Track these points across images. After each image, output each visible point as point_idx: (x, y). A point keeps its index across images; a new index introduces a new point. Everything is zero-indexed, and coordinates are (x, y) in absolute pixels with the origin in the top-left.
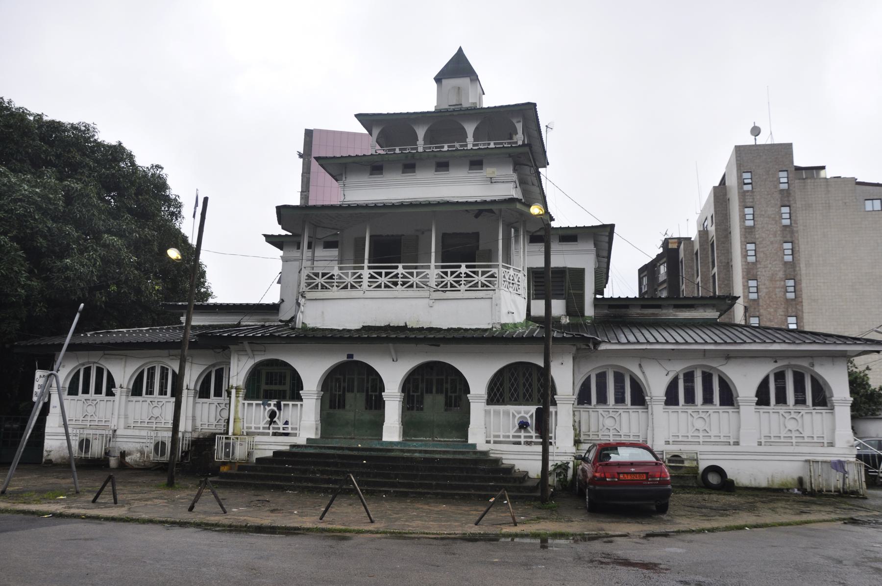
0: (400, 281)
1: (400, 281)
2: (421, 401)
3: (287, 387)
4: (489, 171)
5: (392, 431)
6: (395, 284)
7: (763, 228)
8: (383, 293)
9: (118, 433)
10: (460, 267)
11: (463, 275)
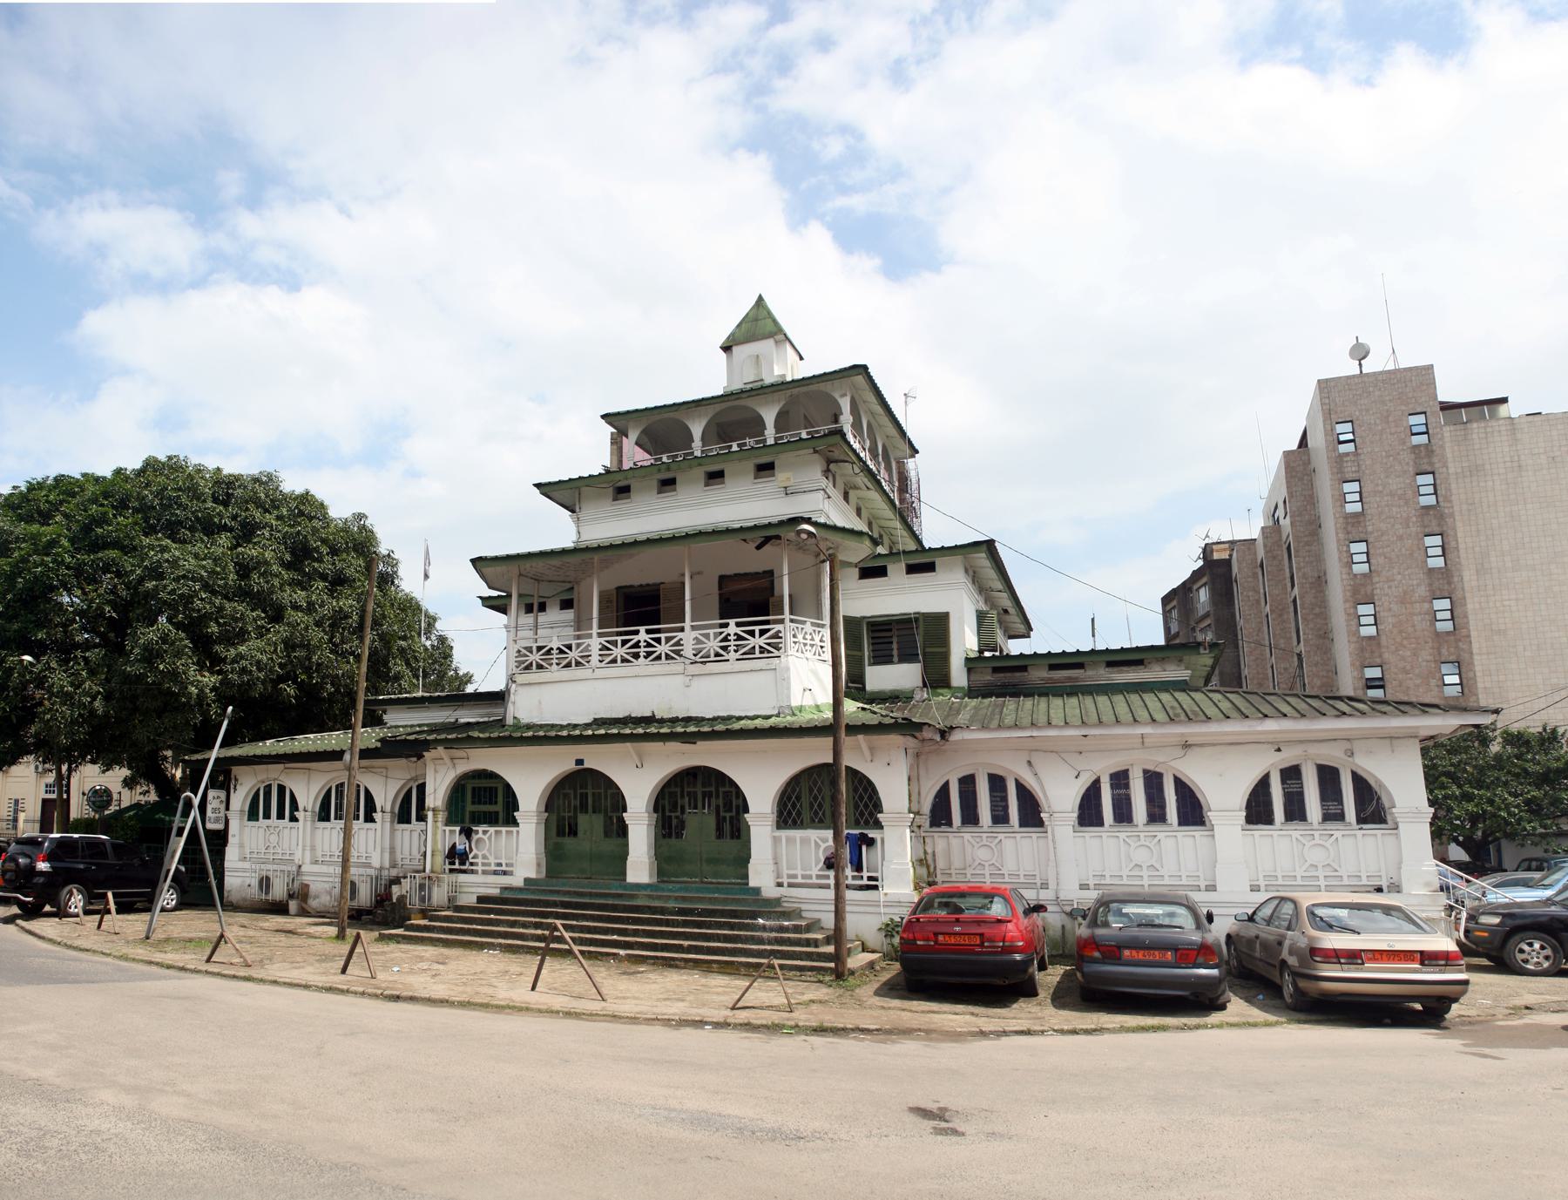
1: (642, 651)
2: (682, 825)
3: (499, 807)
4: (782, 477)
6: (636, 656)
7: (1381, 513)
8: (620, 670)
10: (726, 625)
11: (732, 637)
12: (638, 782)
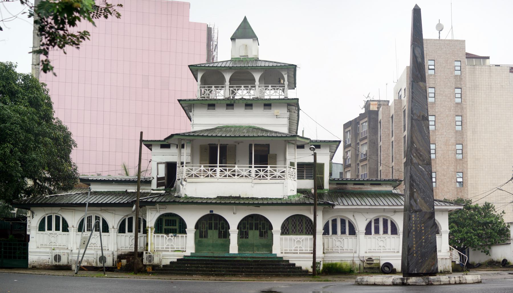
0: (236, 174)
3: (177, 227)
5: (234, 249)
6: (234, 175)
8: (228, 180)
9: (73, 252)
10: (267, 167)
12: (234, 220)
